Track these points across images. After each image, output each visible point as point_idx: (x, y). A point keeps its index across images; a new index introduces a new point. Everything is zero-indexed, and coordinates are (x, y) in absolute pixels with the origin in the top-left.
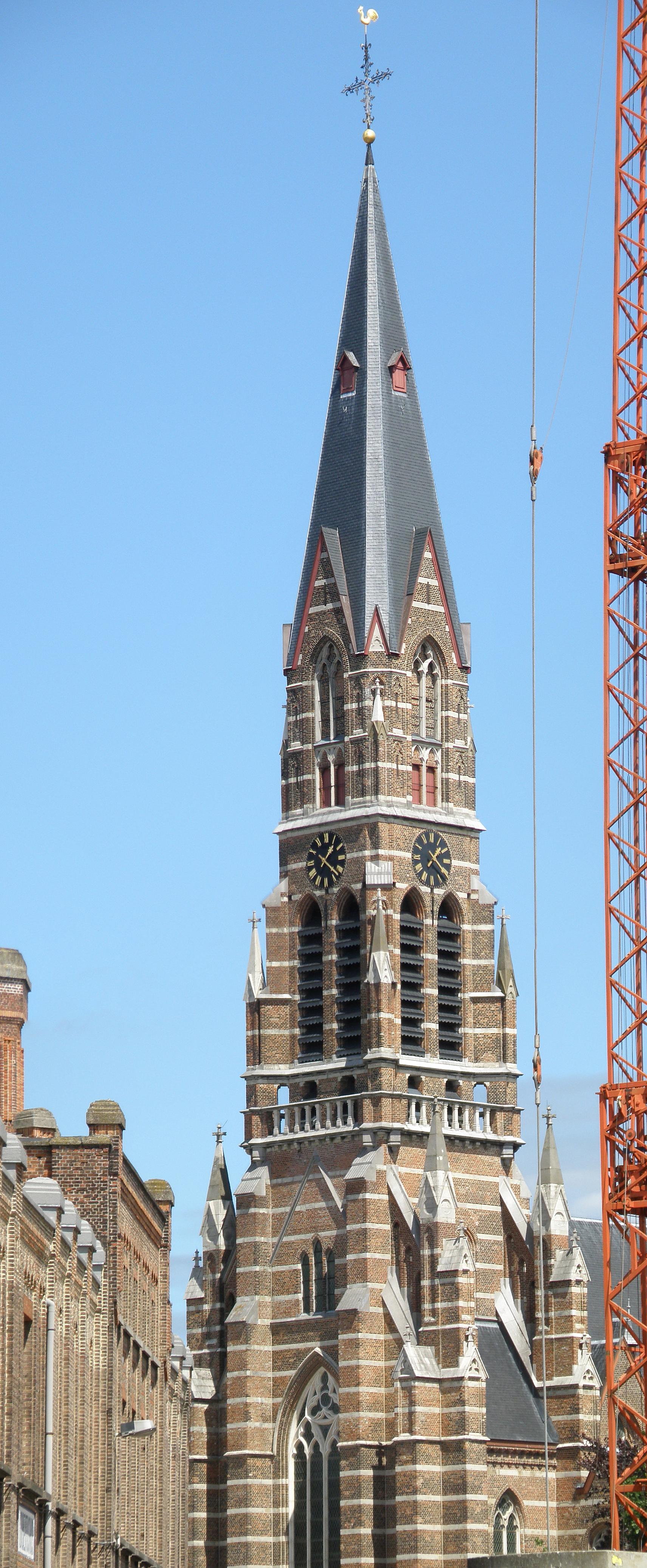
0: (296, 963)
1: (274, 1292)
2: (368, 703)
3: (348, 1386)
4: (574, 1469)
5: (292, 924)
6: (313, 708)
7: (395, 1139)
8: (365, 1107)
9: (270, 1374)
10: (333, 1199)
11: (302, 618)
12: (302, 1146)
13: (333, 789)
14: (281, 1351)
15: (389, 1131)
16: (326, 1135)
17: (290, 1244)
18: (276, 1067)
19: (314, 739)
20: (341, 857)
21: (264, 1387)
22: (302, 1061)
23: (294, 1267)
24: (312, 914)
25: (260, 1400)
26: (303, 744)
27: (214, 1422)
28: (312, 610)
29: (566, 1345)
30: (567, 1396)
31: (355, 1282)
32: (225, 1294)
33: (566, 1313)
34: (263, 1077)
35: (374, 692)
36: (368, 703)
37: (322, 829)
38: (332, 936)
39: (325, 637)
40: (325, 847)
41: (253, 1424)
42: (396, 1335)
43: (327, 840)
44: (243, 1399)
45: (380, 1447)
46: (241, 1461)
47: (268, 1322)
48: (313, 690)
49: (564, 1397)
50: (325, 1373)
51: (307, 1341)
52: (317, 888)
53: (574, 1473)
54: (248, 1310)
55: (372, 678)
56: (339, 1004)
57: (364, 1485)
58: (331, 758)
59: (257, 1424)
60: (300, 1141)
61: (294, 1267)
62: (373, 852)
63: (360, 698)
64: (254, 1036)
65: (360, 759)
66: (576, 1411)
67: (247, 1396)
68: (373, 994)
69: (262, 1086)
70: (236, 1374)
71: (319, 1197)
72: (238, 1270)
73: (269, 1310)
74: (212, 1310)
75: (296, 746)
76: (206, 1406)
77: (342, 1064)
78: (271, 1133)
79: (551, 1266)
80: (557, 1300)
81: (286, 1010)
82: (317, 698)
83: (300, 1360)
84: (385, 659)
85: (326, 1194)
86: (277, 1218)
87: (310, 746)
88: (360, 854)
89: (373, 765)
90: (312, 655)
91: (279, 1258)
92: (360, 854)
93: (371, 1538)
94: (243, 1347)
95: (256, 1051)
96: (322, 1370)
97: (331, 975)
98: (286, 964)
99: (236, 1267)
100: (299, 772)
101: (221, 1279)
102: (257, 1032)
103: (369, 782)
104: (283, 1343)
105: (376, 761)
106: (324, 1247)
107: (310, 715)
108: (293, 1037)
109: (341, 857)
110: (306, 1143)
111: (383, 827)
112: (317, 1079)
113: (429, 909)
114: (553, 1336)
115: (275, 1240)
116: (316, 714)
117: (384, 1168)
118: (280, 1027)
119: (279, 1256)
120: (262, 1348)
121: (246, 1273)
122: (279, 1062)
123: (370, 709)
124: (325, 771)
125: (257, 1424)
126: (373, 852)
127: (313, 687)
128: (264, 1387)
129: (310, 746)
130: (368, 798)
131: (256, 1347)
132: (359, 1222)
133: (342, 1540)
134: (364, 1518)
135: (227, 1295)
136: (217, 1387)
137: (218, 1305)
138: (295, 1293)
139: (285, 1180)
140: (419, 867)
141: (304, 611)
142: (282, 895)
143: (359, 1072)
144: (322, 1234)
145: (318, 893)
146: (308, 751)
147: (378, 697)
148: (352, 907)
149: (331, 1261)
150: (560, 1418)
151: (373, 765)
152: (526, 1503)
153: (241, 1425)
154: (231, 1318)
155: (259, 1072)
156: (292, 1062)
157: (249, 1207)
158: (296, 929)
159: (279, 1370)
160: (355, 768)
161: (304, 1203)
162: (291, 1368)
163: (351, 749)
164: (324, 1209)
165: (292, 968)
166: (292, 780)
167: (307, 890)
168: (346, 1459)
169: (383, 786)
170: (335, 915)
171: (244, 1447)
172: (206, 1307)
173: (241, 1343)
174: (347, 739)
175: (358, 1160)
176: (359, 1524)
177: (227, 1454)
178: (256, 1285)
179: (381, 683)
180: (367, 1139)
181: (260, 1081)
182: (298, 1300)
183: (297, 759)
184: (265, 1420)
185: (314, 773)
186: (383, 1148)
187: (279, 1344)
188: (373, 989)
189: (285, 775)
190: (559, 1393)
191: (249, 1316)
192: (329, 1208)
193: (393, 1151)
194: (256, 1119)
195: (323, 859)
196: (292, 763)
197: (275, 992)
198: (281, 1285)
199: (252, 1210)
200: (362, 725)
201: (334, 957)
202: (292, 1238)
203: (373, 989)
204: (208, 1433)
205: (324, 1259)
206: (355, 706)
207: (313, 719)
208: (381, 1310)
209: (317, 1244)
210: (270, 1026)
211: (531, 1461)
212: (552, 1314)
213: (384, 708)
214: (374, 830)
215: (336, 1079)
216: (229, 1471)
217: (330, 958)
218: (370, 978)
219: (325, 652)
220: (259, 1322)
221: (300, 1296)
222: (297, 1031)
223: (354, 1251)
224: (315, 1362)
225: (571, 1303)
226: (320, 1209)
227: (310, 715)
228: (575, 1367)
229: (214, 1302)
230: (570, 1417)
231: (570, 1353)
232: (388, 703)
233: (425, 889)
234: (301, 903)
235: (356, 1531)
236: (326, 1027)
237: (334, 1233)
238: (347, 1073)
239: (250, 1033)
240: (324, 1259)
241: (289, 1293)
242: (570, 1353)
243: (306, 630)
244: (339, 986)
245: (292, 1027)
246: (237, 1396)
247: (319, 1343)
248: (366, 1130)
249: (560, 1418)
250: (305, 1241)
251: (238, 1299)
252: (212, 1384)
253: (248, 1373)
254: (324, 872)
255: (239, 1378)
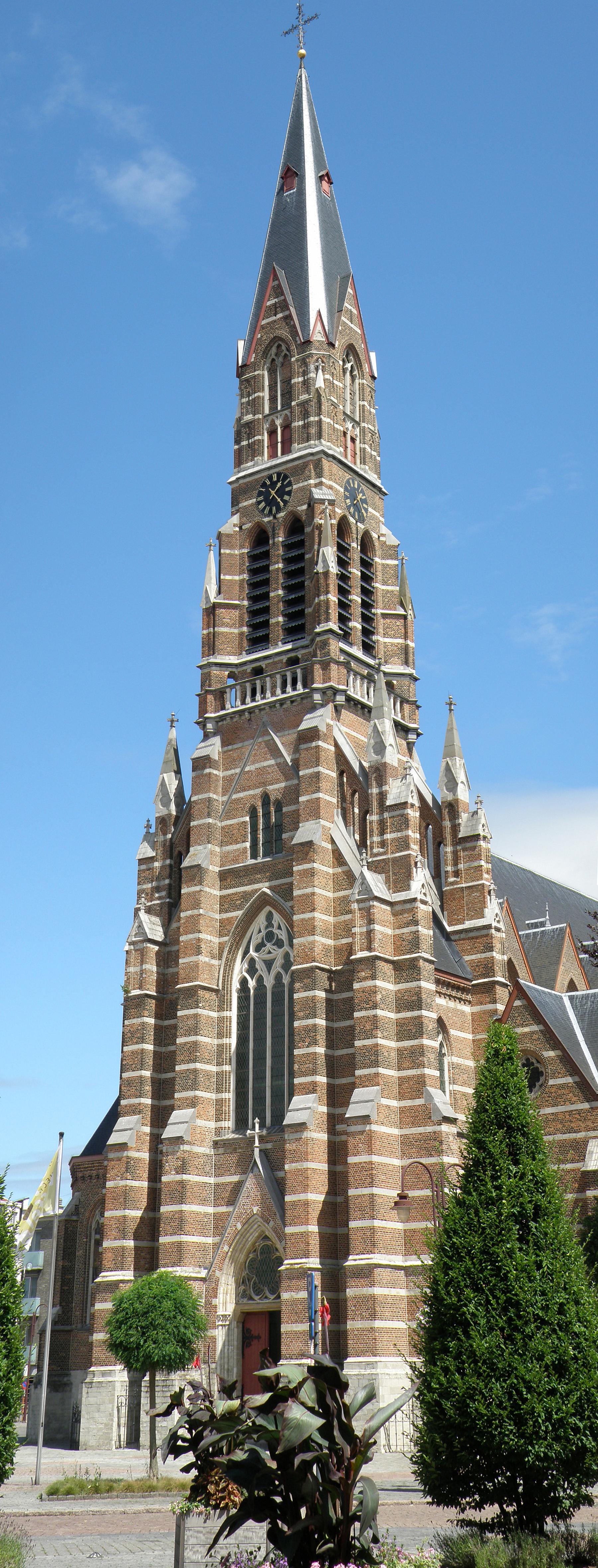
0: (246, 576)
1: (222, 844)
2: (312, 375)
3: (303, 913)
4: (490, 1003)
5: (242, 547)
6: (263, 390)
7: (341, 699)
8: (315, 671)
9: (217, 916)
10: (282, 756)
11: (255, 328)
12: (252, 715)
13: (279, 445)
14: (229, 895)
15: (336, 692)
16: (275, 701)
17: (238, 800)
18: (227, 657)
19: (263, 411)
20: (287, 489)
21: (213, 927)
22: (249, 653)
23: (242, 819)
24: (260, 538)
25: (210, 938)
26: (254, 415)
27: (162, 963)
28: (264, 322)
29: (477, 891)
30: (482, 937)
31: (308, 820)
32: (176, 850)
33: (476, 864)
34: (216, 664)
35: (317, 369)
36: (312, 375)
37: (271, 472)
38: (279, 550)
39: (275, 337)
40: (273, 485)
41: (203, 959)
42: (345, 868)
43: (275, 479)
44: (196, 935)
45: (329, 971)
46: (192, 992)
47: (217, 869)
48: (263, 378)
49: (477, 938)
50: (270, 912)
51: (254, 883)
52: (266, 516)
53: (490, 1007)
54: (203, 855)
55: (315, 358)
56: (285, 602)
57: (318, 1005)
58: (278, 422)
59: (207, 959)
60: (251, 711)
61: (242, 819)
62: (317, 481)
63: (305, 373)
64: (209, 634)
65: (306, 415)
66: (491, 949)
67: (200, 932)
68: (322, 581)
69: (215, 671)
70: (189, 913)
71: (268, 756)
72: (192, 824)
73: (218, 859)
74: (162, 867)
75: (249, 417)
76: (157, 948)
77: (289, 646)
78: (223, 708)
79: (459, 824)
80: (466, 853)
81: (236, 613)
82: (267, 383)
83: (247, 901)
84: (326, 347)
85: (275, 752)
86: (228, 780)
87: (260, 416)
88: (306, 483)
89: (317, 419)
90: (264, 352)
91: (228, 814)
92: (306, 483)
93: (323, 1057)
94: (197, 888)
95: (210, 645)
96: (268, 908)
97: (278, 579)
98: (237, 578)
99: (190, 821)
100: (250, 436)
101: (171, 839)
102: (211, 630)
103: (313, 431)
104: (231, 888)
105: (319, 415)
106: (272, 798)
107: (261, 394)
108: (241, 634)
109: (287, 489)
110: (257, 711)
111: (326, 464)
112: (263, 664)
113: (355, 536)
114: (464, 885)
115: (225, 798)
116: (266, 394)
117: (331, 723)
118: (231, 627)
119: (229, 811)
120: (212, 891)
121: (200, 825)
122: (229, 654)
123: (315, 380)
124: (272, 433)
125: (207, 959)
126: (317, 481)
127: (263, 375)
128: (213, 927)
129: (260, 416)
130: (312, 442)
131: (207, 889)
132: (312, 767)
133: (296, 1060)
134: (318, 1037)
135: (175, 853)
136: (165, 933)
137: (168, 862)
138: (243, 842)
139: (235, 746)
140: (348, 501)
141: (257, 322)
142: (235, 525)
143: (304, 651)
144: (270, 788)
145: (266, 520)
146: (259, 419)
147: (320, 371)
148: (297, 527)
149: (279, 809)
150: (473, 957)
151: (317, 419)
152: (452, 1032)
153: (193, 959)
154: (186, 863)
155: (212, 660)
156: (241, 654)
157: (204, 768)
158: (246, 551)
159: (226, 912)
160: (301, 423)
161: (253, 763)
162: (238, 909)
163: (297, 410)
164: (273, 765)
165: (242, 581)
166: (244, 443)
167: (257, 519)
168: (301, 981)
169: (325, 434)
170: (281, 534)
171: (196, 979)
172: (157, 864)
173: (196, 885)
174: (293, 403)
175: (308, 716)
176: (315, 1043)
177: (178, 986)
178: (208, 835)
179: (323, 362)
180: (317, 697)
181: (214, 668)
182: (246, 848)
183: (249, 427)
184: (213, 957)
185: (263, 434)
186: (330, 706)
187: (226, 889)
188: (322, 576)
189: (237, 441)
190: (471, 935)
191: (203, 861)
192: (278, 765)
193: (337, 709)
194: (210, 698)
195: (273, 492)
196: (244, 430)
197: (227, 599)
198: (229, 836)
199: (207, 771)
200: (308, 391)
201: (281, 565)
202: (241, 795)
203: (322, 576)
204: (157, 973)
205: (272, 809)
206: (301, 379)
207: (263, 397)
208: (329, 846)
209: (266, 798)
210: (223, 625)
211: (454, 993)
212: (461, 866)
213: (324, 380)
214: (318, 466)
215: (281, 661)
216: (180, 1002)
217: (276, 566)
218: (320, 568)
219: (274, 350)
220: (211, 868)
221: (248, 844)
222: (245, 629)
223: (307, 792)
224: (264, 901)
225: (480, 855)
226: (269, 766)
227: (261, 394)
228: (486, 910)
229: (164, 859)
230: (484, 955)
231: (481, 899)
232: (328, 376)
233: (352, 520)
234: (250, 530)
235: (311, 1050)
236: (273, 621)
237: (283, 785)
238: (292, 655)
239: (205, 632)
240: (272, 809)
241: (237, 843)
242: (481, 899)
243: (259, 336)
244: (284, 588)
245: (241, 626)
246: (190, 933)
247: (267, 884)
248: (317, 690)
249: (473, 957)
250: (253, 796)
251: (191, 849)
252: (161, 930)
253: (201, 911)
254: (271, 502)
255: (193, 916)
